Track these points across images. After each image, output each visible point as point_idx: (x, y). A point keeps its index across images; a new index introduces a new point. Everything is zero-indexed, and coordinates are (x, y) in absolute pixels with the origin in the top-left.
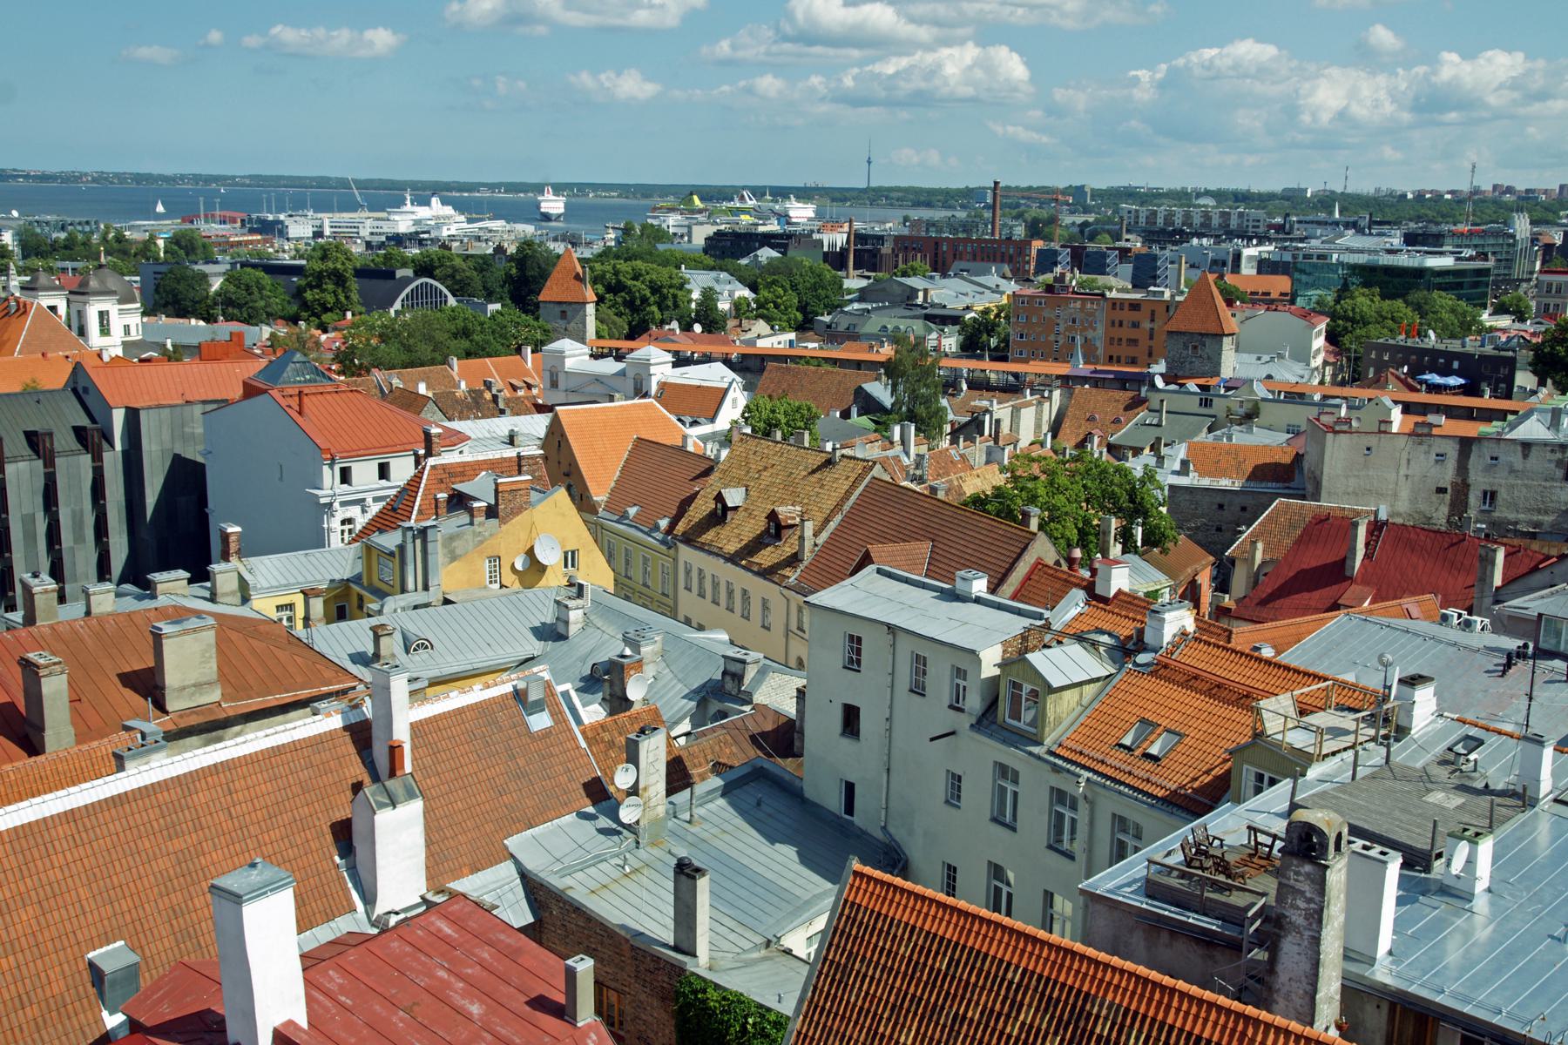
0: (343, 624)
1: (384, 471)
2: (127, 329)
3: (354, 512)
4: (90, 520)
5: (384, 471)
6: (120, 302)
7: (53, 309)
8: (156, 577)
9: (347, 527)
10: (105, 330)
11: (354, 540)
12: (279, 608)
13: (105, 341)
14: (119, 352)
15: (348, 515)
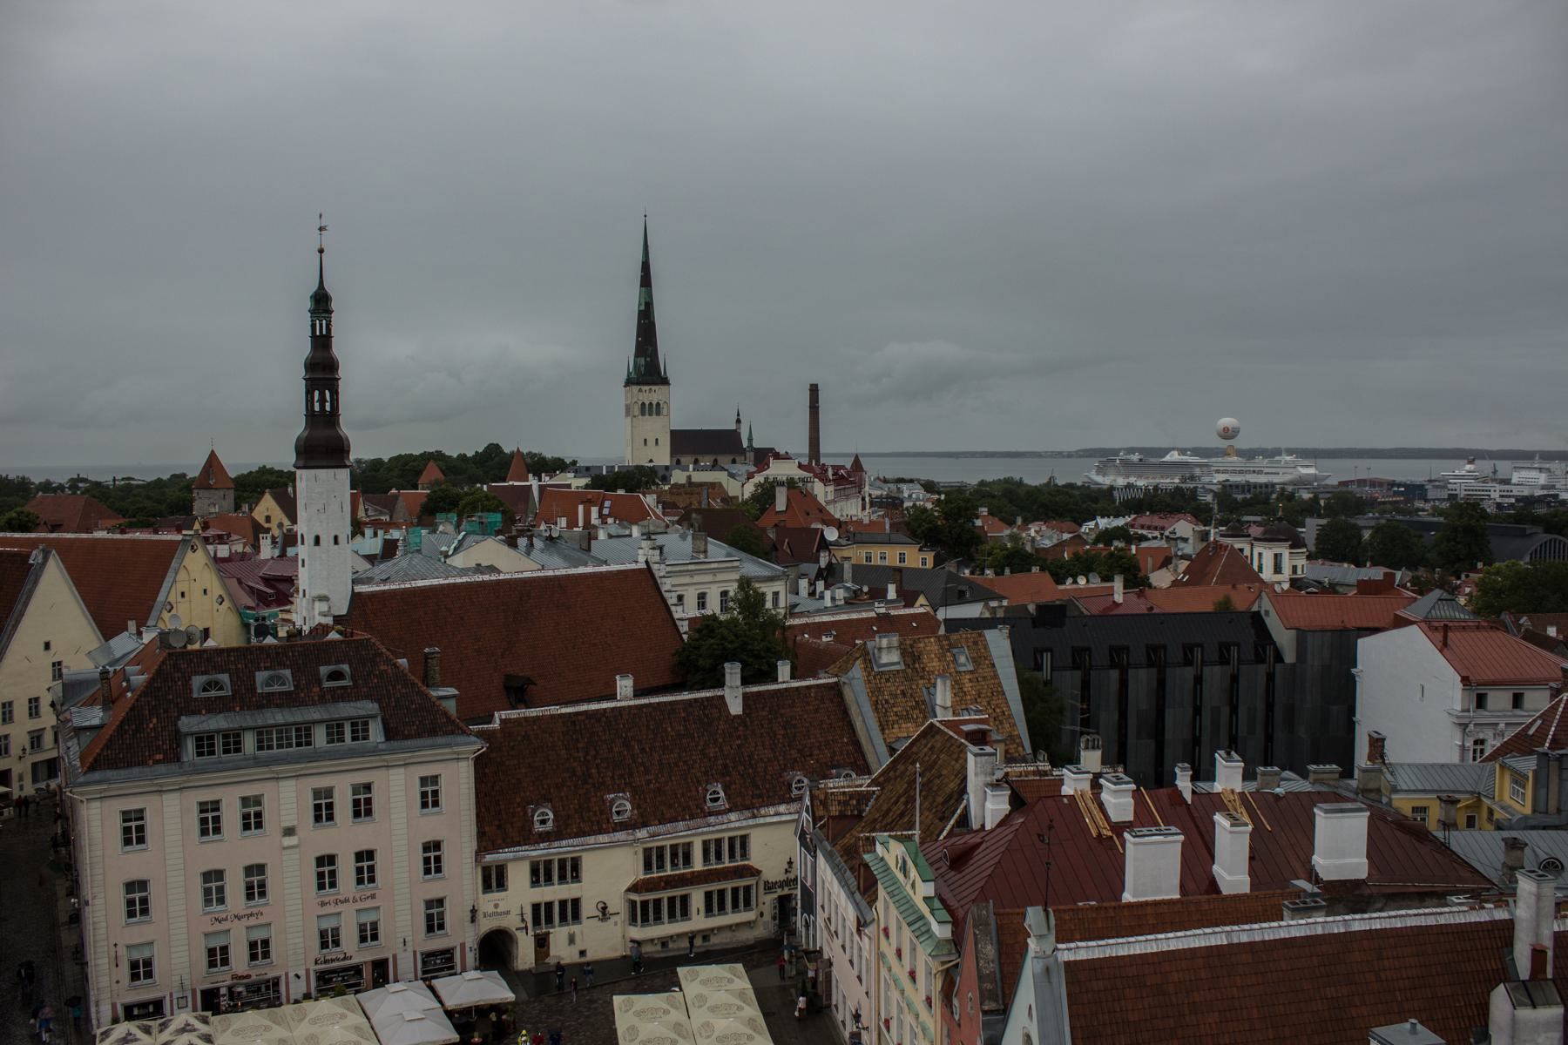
0: (1475, 833)
1: (1517, 701)
2: (1294, 568)
3: (1487, 735)
4: (1260, 715)
5: (1517, 701)
6: (1291, 547)
7: (1241, 550)
8: (1312, 767)
9: (1479, 747)
10: (1278, 569)
11: (1489, 759)
12: (1415, 809)
13: (1277, 577)
14: (1286, 586)
15: (1481, 736)
